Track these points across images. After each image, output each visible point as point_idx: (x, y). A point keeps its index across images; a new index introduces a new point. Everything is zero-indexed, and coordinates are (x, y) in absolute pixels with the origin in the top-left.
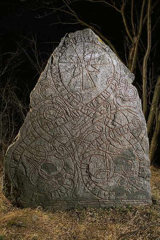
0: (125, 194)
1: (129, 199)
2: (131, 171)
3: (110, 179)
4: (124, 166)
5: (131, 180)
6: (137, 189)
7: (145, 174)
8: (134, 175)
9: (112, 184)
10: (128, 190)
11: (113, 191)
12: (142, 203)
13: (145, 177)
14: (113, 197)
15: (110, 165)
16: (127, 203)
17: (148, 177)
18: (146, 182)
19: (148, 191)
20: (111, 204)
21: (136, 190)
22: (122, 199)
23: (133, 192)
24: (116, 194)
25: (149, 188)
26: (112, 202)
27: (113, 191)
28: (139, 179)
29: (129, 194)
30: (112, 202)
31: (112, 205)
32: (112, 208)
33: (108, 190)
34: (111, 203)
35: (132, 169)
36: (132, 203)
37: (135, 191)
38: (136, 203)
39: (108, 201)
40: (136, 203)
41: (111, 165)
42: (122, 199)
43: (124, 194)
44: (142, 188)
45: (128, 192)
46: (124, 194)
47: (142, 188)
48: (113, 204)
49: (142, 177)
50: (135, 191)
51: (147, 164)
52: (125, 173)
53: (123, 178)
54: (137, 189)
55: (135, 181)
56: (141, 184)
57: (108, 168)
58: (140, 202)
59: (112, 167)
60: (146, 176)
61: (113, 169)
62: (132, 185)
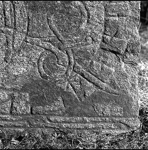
0: (60, 99)
1: (71, 115)
2: (79, 31)
3: (14, 55)
4: (56, 17)
5: (80, 61)
6: (97, 86)
7: (121, 43)
8: (88, 44)
9: (22, 70)
10: (68, 87)
11: (24, 89)
12: (111, 128)
13: (122, 52)
14: (22, 107)
15: (15, 12)
16: (64, 125)
17: (133, 52)
18: (126, 67)
19: (130, 93)
20: (19, 127)
21: (94, 89)
22: (52, 113)
23: (85, 95)
24: (32, 99)
25: (133, 85)
26: (20, 120)
27: (24, 89)
28: (102, 58)
29: (71, 100)
30: (20, 120)
31: (22, 130)
32: (20, 139)
33: (8, 87)
34: (17, 124)
35: (83, 27)
36: (80, 126)
37: (89, 93)
38: (91, 126)
39: (9, 117)
40: (91, 126)
41: (18, 12)
42: (52, 113)
43: (56, 100)
44: (112, 84)
45: (69, 95)
46: (56, 100)
47: (112, 84)
48: (24, 126)
49: (113, 52)
50: (89, 93)
51: (130, 13)
52: (61, 37)
53: (53, 52)
54: (97, 86)
55: (92, 63)
56: (110, 73)
57: (9, 22)
58: (104, 125)
59: (19, 20)
60: (126, 51)
61: (24, 26)
62: (82, 75)
